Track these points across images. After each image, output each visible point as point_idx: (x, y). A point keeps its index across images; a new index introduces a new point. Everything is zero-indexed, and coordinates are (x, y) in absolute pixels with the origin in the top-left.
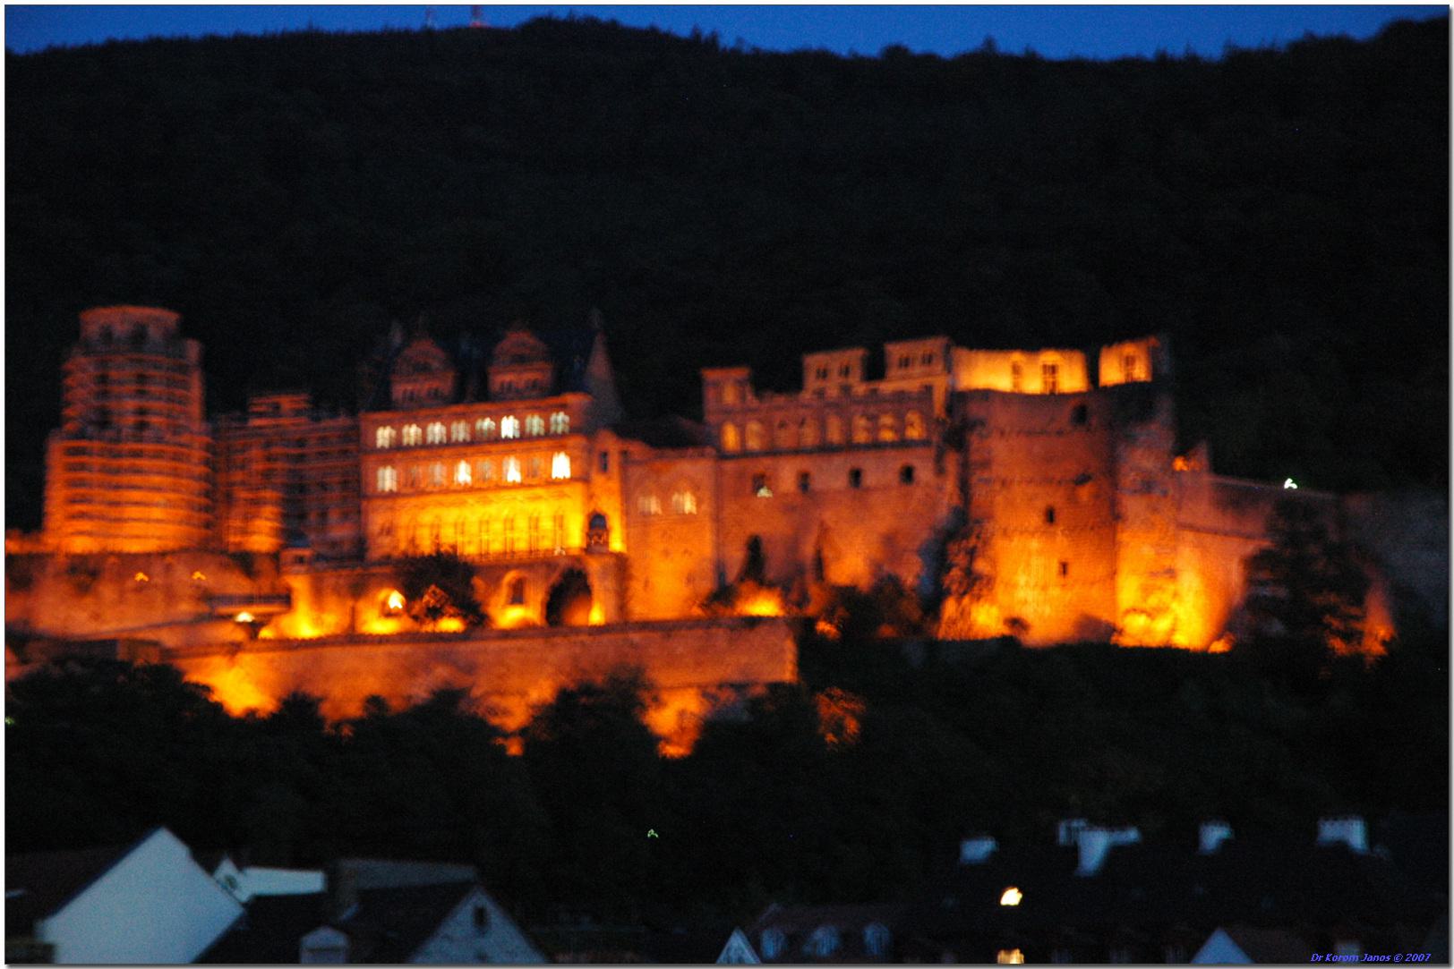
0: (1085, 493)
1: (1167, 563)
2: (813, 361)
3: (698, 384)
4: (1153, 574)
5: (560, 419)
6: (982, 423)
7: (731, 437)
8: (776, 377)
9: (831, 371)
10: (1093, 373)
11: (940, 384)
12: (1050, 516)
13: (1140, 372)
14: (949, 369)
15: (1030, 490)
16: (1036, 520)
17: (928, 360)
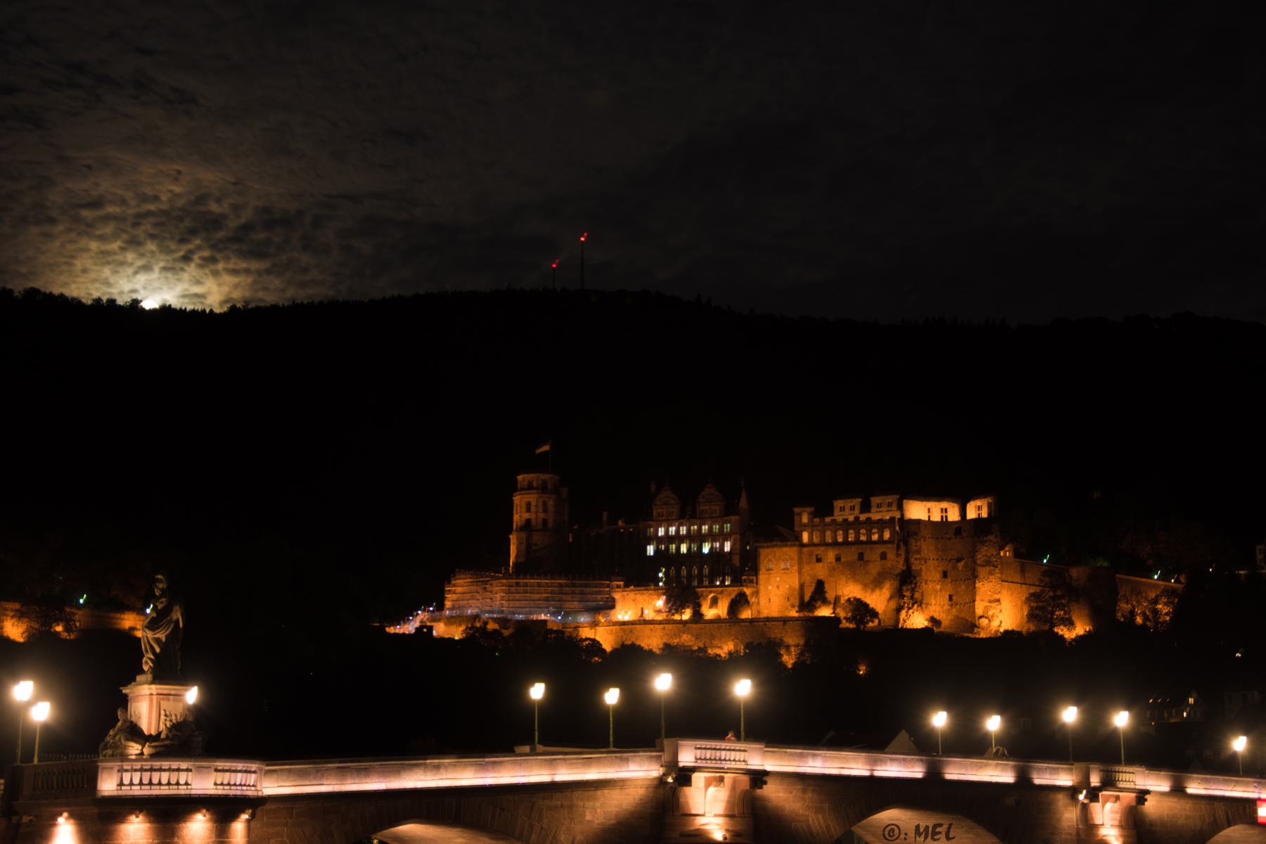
0: (960, 565)
1: (997, 596)
2: (838, 504)
3: (792, 515)
4: (990, 602)
5: (727, 527)
6: (916, 534)
7: (805, 537)
8: (822, 509)
9: (846, 509)
10: (963, 512)
11: (898, 515)
12: (945, 575)
13: (984, 514)
14: (900, 508)
15: (936, 563)
16: (938, 576)
17: (890, 505)
